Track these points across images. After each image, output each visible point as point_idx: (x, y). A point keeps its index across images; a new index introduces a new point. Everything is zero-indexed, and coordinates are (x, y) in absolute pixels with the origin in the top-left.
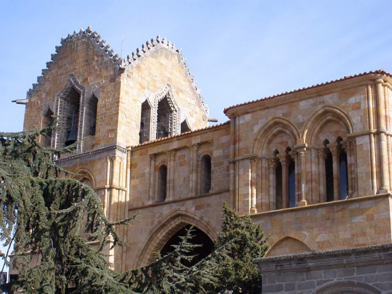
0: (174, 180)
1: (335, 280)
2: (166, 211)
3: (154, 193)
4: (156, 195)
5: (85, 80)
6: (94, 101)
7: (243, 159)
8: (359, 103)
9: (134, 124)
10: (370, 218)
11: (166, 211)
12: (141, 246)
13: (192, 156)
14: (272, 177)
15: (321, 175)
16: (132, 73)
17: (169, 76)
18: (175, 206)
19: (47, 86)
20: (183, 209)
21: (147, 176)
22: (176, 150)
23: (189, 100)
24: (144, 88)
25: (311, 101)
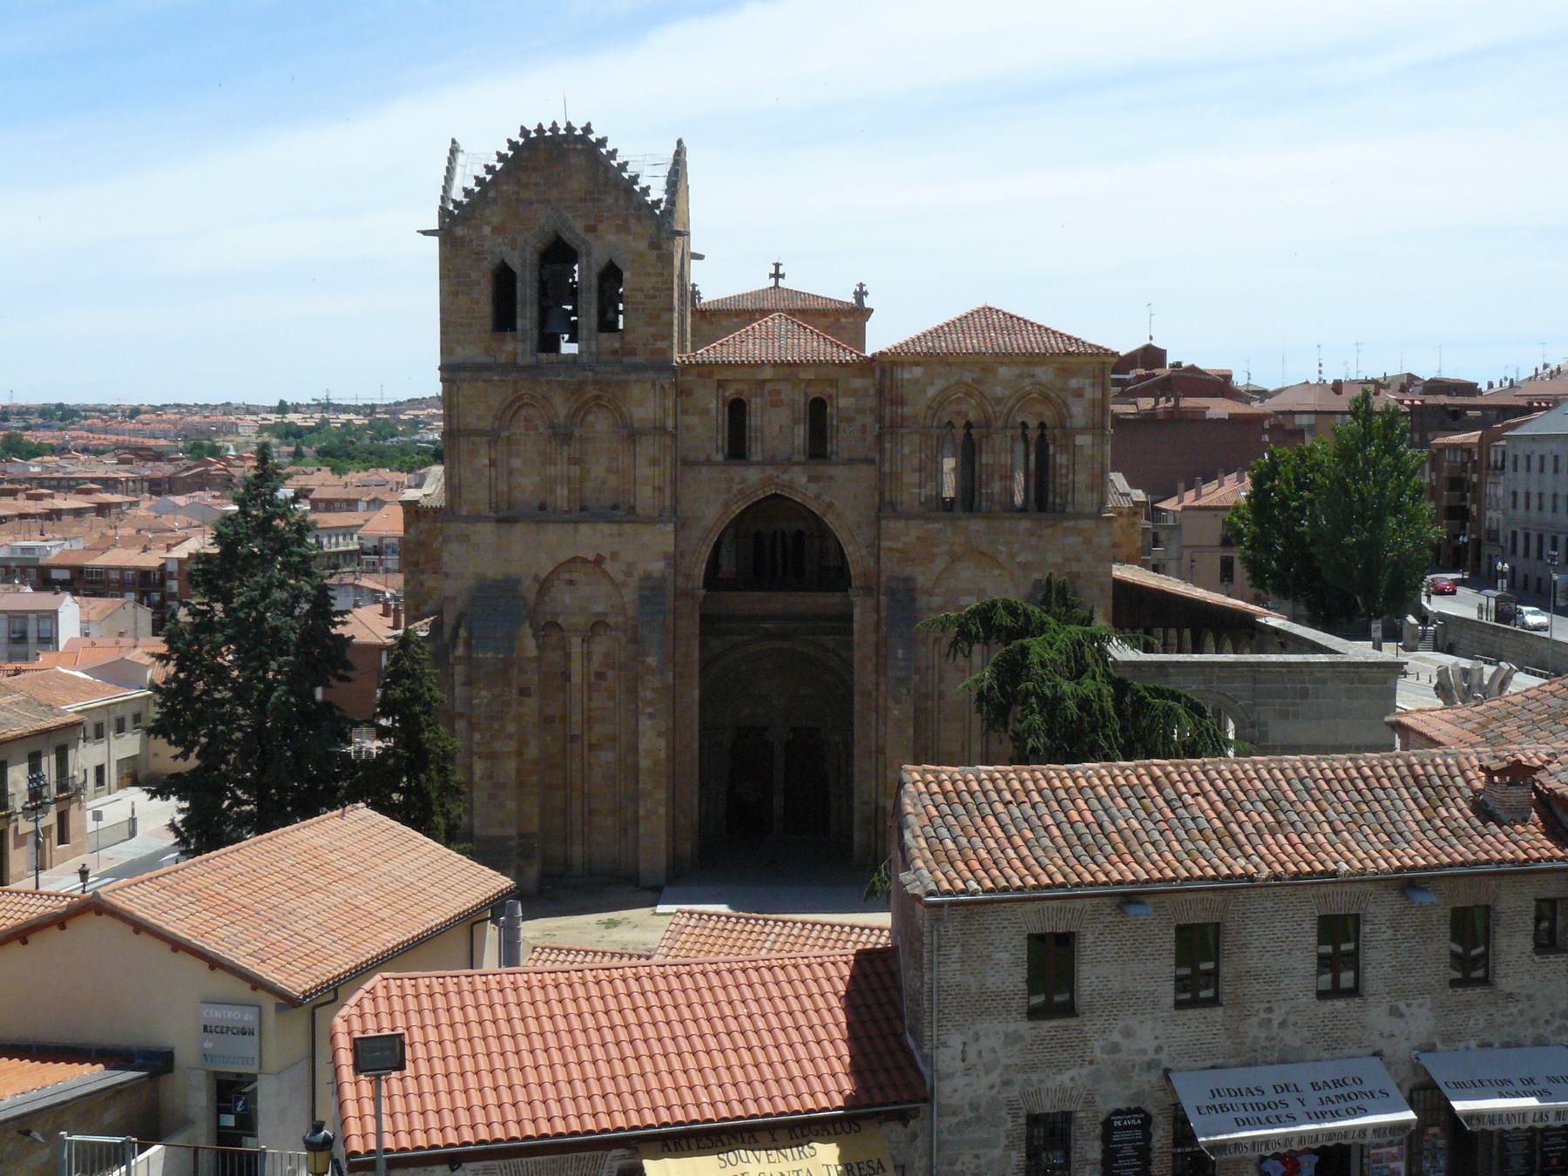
1: (1194, 687)
2: (753, 475)
4: (726, 446)
5: (591, 229)
6: (611, 275)
7: (911, 433)
10: (1087, 542)
11: (752, 478)
13: (799, 398)
18: (769, 471)
19: (494, 215)
20: (786, 477)
21: (714, 413)
22: (765, 381)
25: (1015, 370)
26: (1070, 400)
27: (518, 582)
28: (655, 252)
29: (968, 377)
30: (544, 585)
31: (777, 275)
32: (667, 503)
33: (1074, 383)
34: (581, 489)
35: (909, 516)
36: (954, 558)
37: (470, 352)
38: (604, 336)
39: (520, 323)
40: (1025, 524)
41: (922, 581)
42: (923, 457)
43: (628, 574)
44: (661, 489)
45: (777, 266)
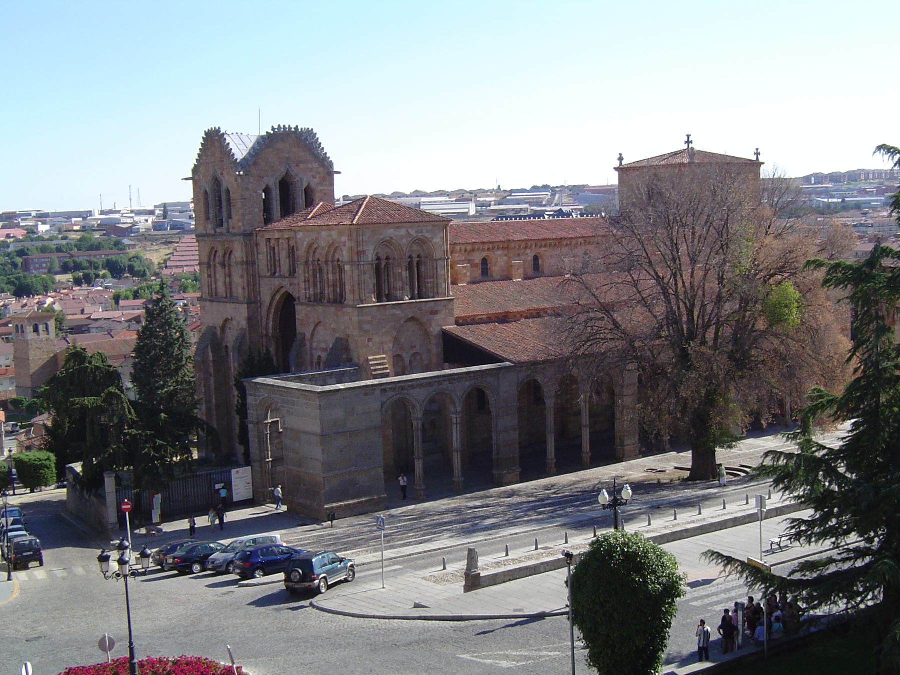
0: (280, 260)
1: (266, 395)
2: (277, 282)
3: (271, 266)
5: (222, 174)
6: (228, 192)
8: (345, 242)
9: (257, 210)
10: (351, 319)
12: (268, 304)
14: (318, 276)
15: (338, 281)
16: (250, 172)
17: (287, 156)
21: (266, 254)
23: (310, 166)
24: (263, 178)
26: (343, 248)
27: (216, 328)
28: (236, 183)
29: (314, 237)
30: (223, 328)
31: (688, 142)
32: (247, 295)
33: (344, 239)
34: (231, 289)
35: (303, 304)
36: (317, 326)
37: (201, 230)
38: (230, 220)
39: (211, 216)
40: (332, 310)
41: (308, 336)
42: (307, 275)
43: (238, 326)
44: (244, 289)
45: (689, 136)
